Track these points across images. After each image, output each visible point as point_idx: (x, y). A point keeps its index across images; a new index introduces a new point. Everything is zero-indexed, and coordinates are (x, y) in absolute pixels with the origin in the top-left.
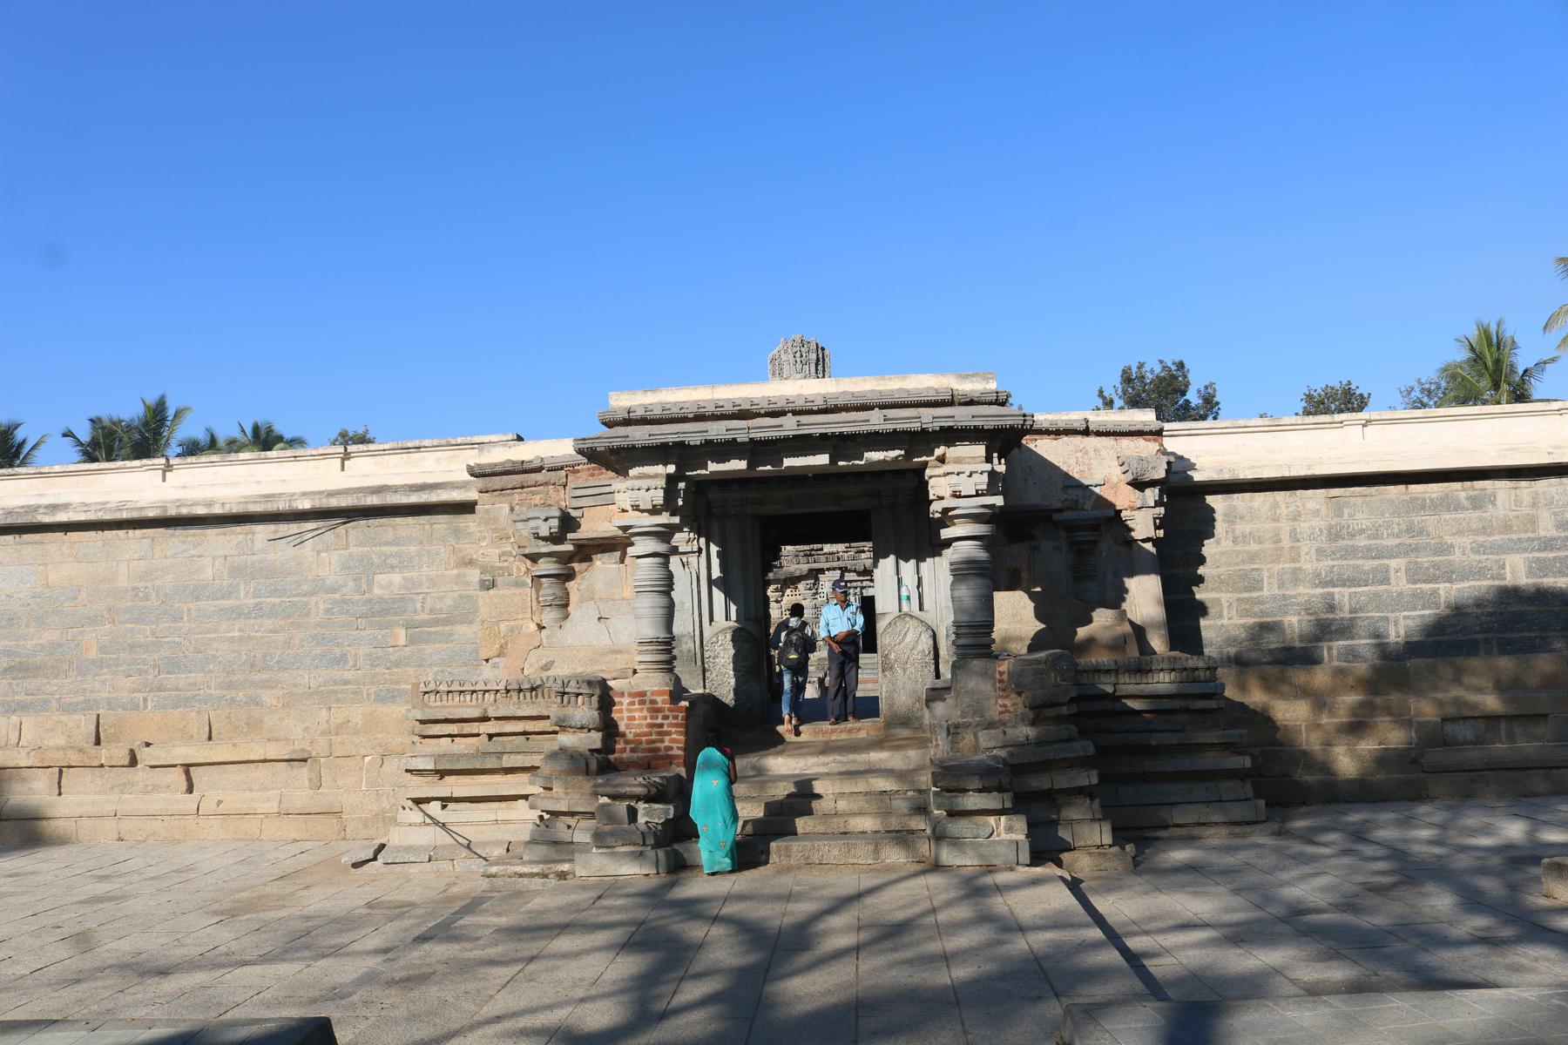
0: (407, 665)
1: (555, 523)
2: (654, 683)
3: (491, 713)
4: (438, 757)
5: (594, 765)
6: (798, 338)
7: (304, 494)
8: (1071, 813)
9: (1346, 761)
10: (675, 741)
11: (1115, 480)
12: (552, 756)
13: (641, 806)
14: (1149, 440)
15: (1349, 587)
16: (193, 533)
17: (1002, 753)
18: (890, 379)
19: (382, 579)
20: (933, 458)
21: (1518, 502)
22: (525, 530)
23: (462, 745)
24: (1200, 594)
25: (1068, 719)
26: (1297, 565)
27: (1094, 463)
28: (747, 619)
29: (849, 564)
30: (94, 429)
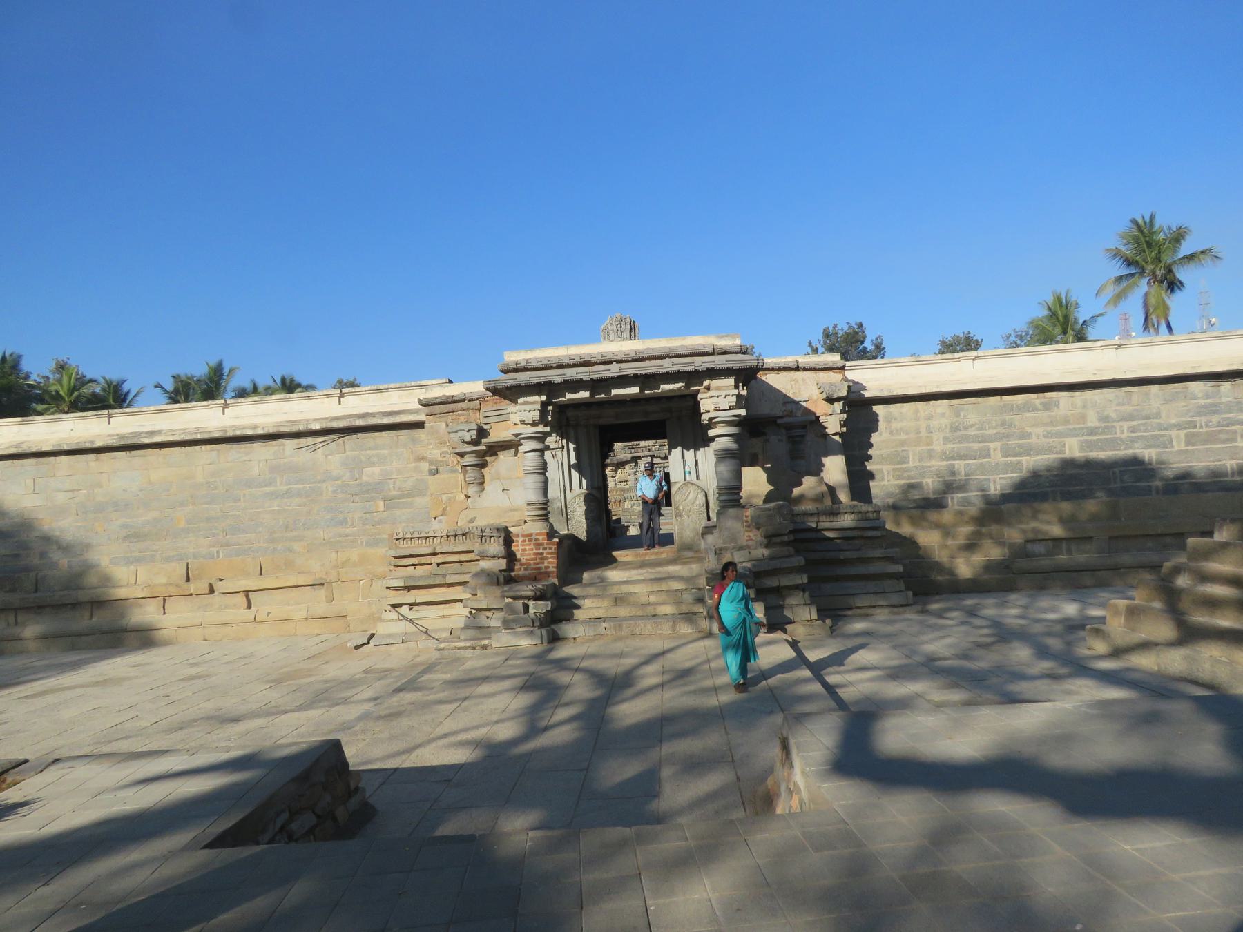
0: (385, 523)
1: (474, 433)
2: (537, 528)
3: (438, 550)
4: (406, 579)
5: (502, 579)
6: (618, 315)
7: (316, 420)
8: (791, 601)
9: (965, 568)
10: (551, 564)
11: (815, 397)
12: (477, 575)
13: (531, 603)
14: (836, 373)
15: (965, 460)
17: (749, 565)
18: (675, 340)
19: (367, 470)
20: (703, 387)
21: (1074, 405)
22: (456, 438)
23: (420, 571)
24: (870, 466)
25: (788, 543)
26: (931, 447)
28: (593, 488)
29: (656, 453)
30: (175, 382)
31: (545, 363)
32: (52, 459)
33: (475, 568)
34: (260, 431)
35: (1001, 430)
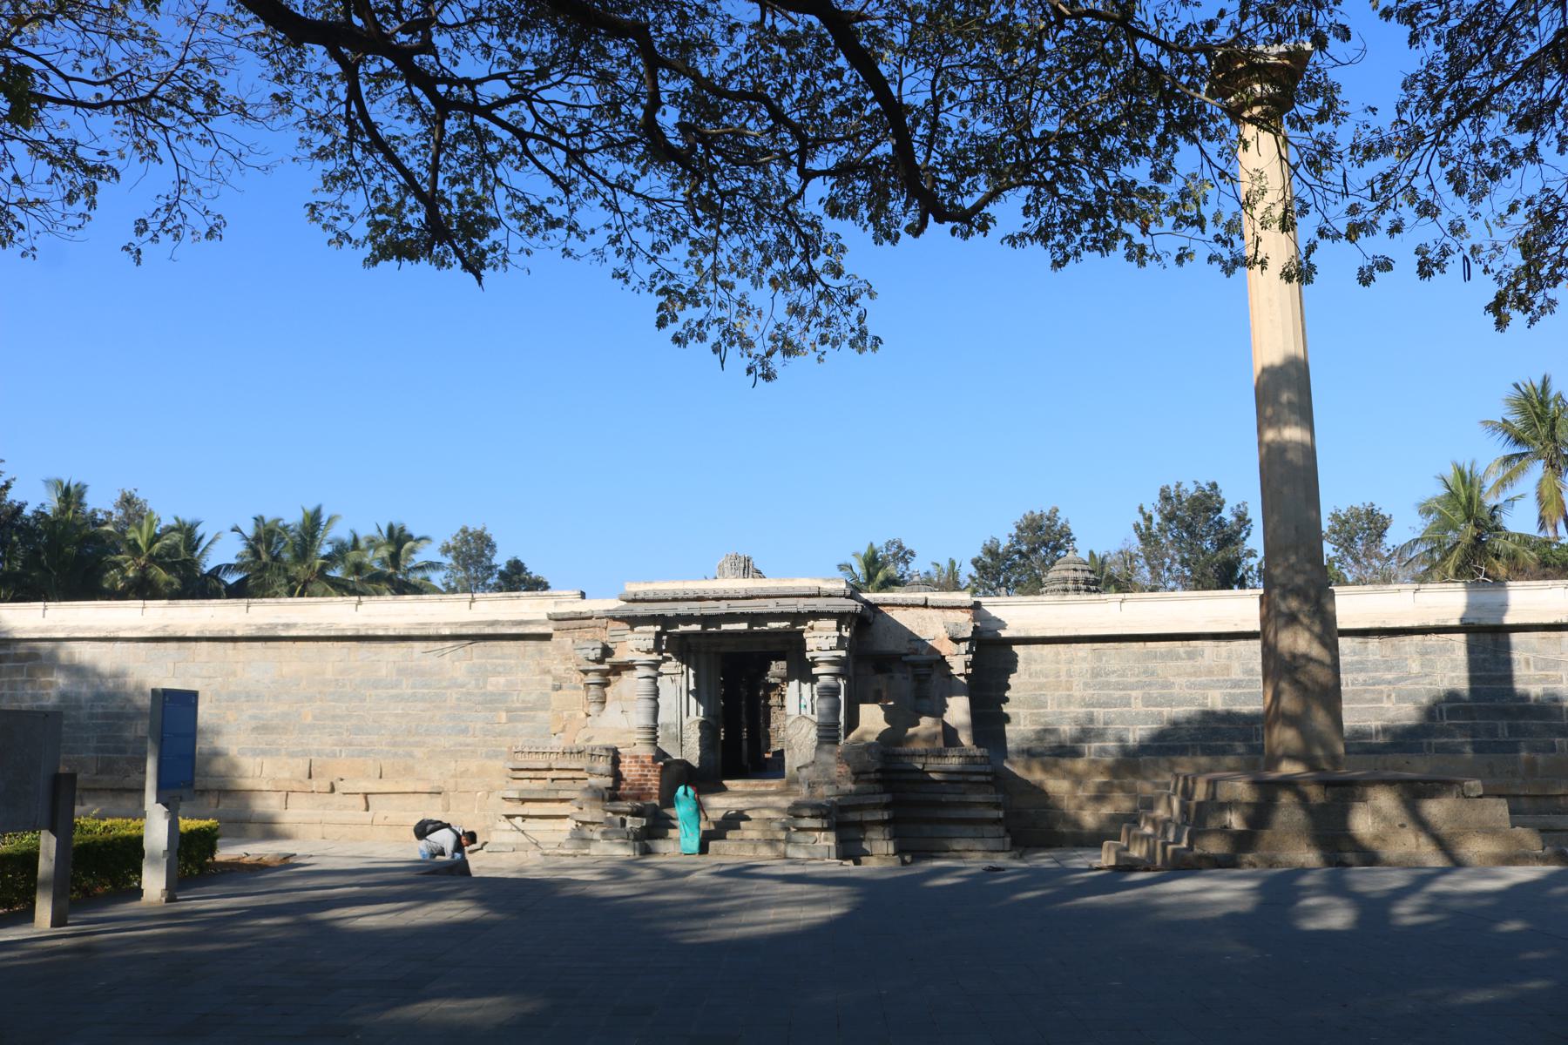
2: (645, 751)
3: (554, 766)
4: (522, 791)
5: (607, 796)
7: (446, 624)
8: (870, 835)
9: (1089, 819)
10: (653, 783)
12: (585, 790)
13: (629, 818)
16: (374, 645)
17: (835, 799)
19: (493, 680)
22: (581, 654)
23: (536, 784)
24: (1006, 709)
25: (878, 781)
30: (257, 526)
31: (661, 596)
32: (193, 644)
33: (585, 784)
34: (391, 633)
35: (1143, 678)
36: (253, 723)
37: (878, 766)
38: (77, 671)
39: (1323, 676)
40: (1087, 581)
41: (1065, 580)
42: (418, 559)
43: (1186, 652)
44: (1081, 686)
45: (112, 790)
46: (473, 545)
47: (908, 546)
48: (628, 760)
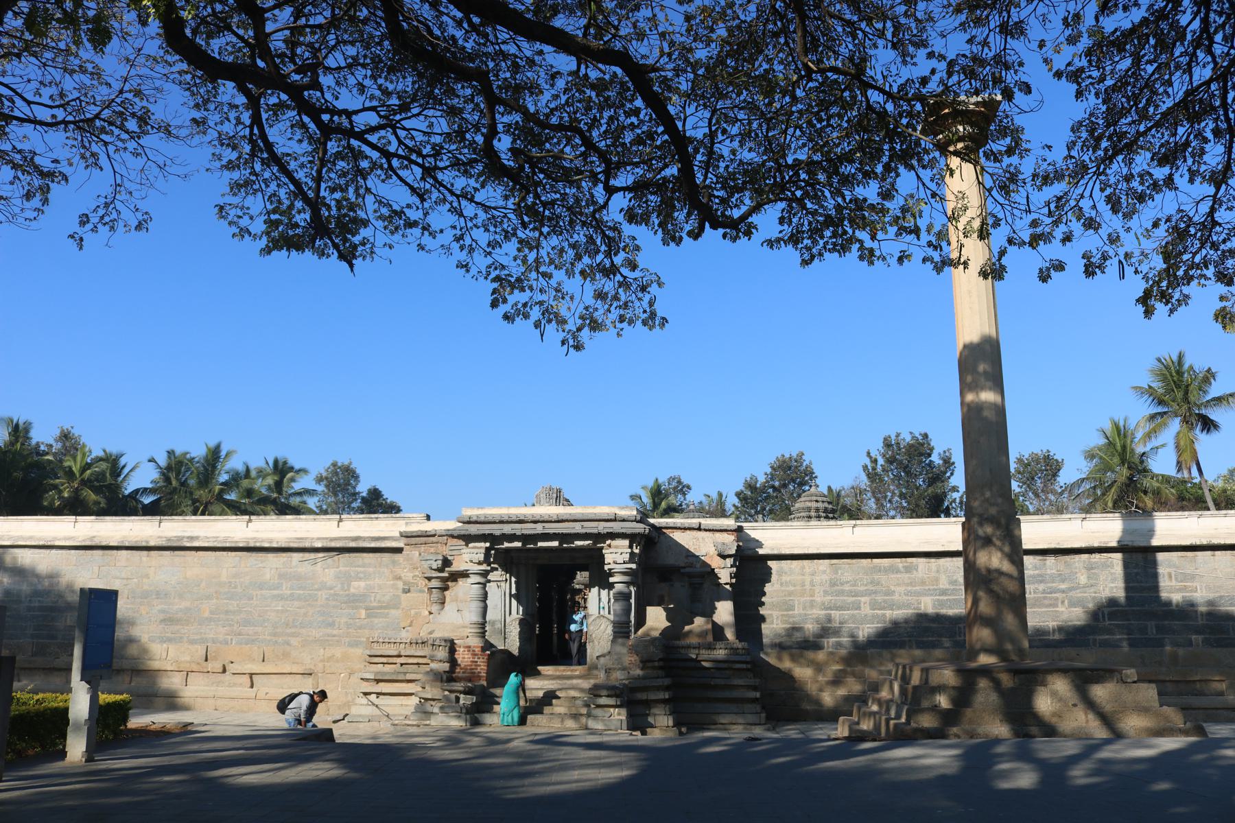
2: (476, 642)
3: (402, 654)
4: (376, 673)
5: (445, 678)
7: (319, 539)
9: (828, 699)
10: (482, 668)
11: (711, 553)
13: (462, 696)
17: (627, 682)
19: (355, 584)
21: (929, 570)
22: (426, 565)
23: (388, 668)
24: (762, 611)
25: (661, 668)
27: (702, 545)
30: (169, 458)
31: (490, 519)
33: (427, 668)
34: (275, 545)
35: (870, 587)
36: (162, 616)
37: (661, 656)
38: (20, 572)
39: (1012, 586)
40: (826, 510)
41: (809, 509)
42: (297, 486)
43: (905, 567)
44: (822, 593)
45: (44, 669)
46: (341, 476)
47: (685, 481)
48: (462, 650)
